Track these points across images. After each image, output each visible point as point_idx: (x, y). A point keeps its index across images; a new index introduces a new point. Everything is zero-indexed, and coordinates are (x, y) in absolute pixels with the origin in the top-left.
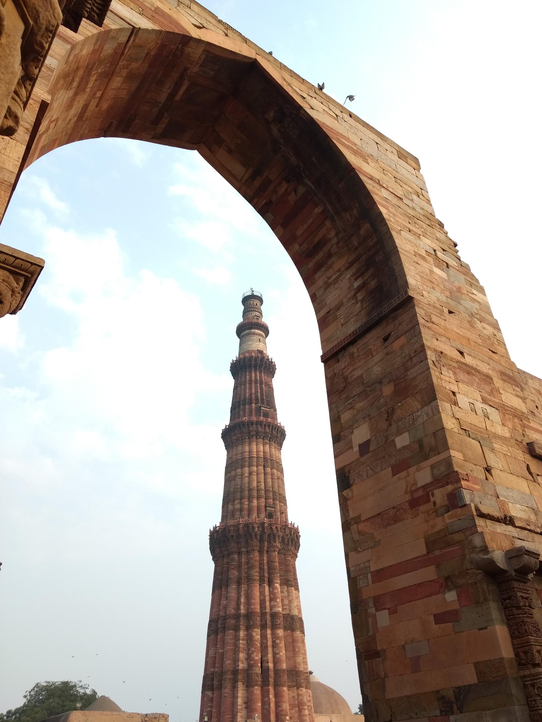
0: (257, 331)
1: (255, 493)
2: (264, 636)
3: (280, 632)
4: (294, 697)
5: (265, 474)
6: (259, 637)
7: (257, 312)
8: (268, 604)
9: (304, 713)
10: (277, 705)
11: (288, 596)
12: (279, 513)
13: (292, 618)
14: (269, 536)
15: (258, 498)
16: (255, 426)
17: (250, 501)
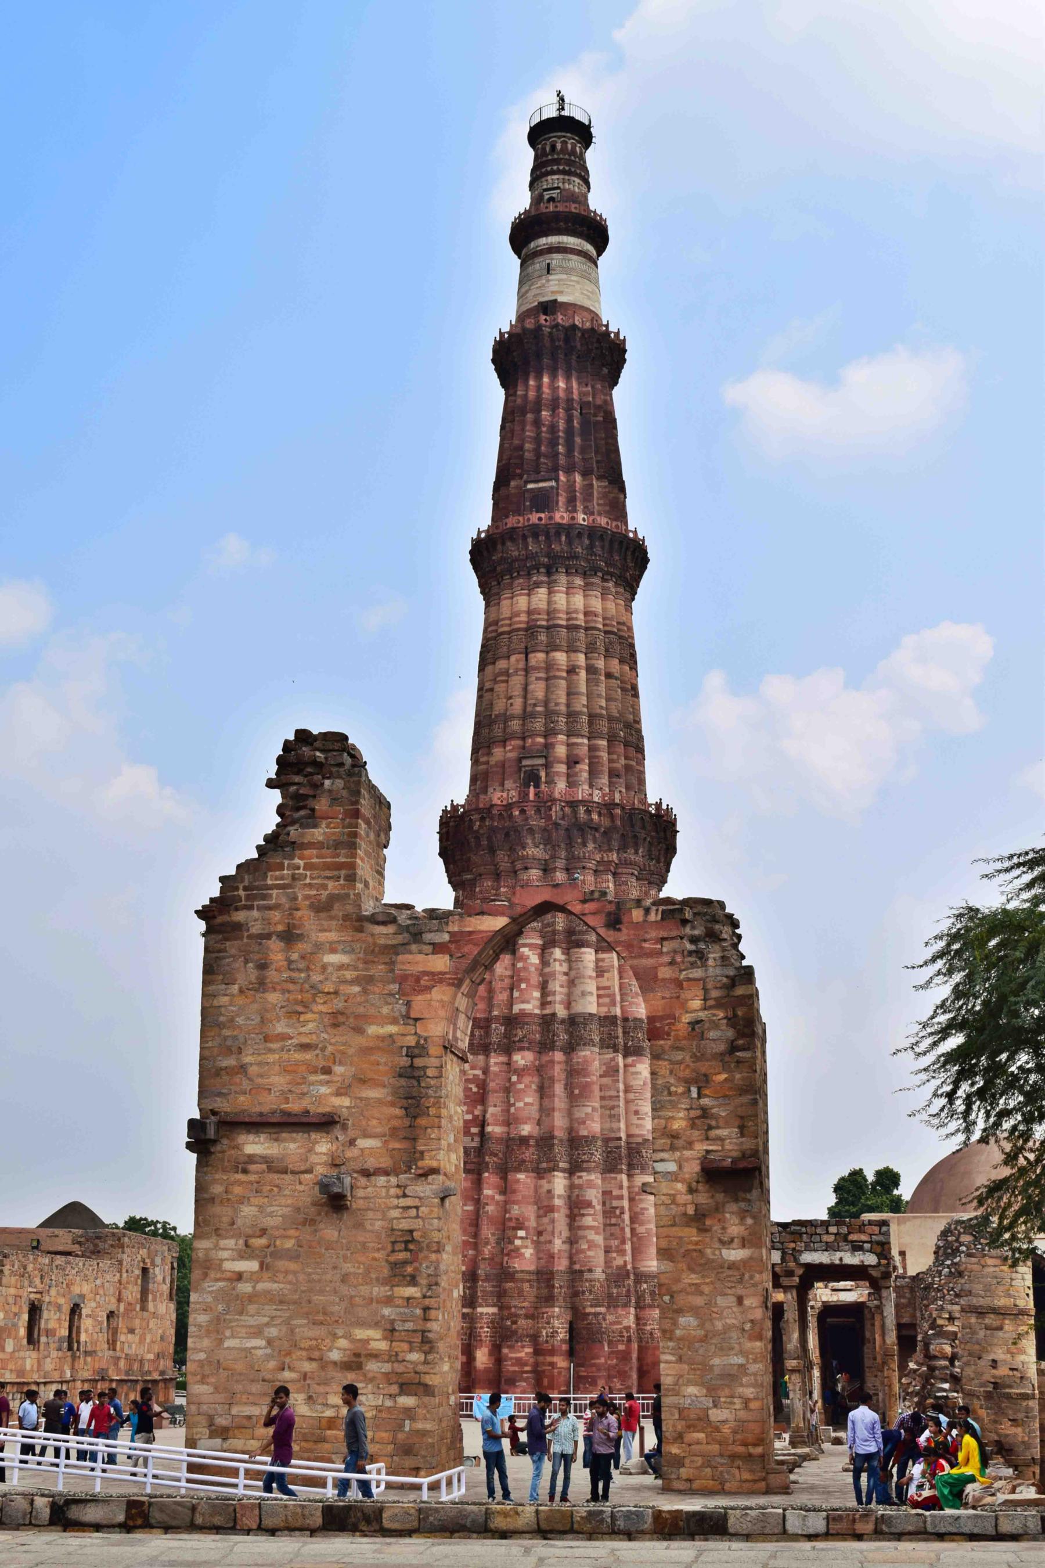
0: (543, 241)
1: (498, 731)
2: (486, 1071)
3: (521, 1059)
4: (549, 1191)
5: (527, 670)
6: (478, 1072)
7: (553, 173)
8: (502, 997)
9: (580, 1224)
10: (505, 1207)
11: (570, 968)
12: (562, 768)
13: (573, 1022)
14: (507, 835)
15: (504, 743)
16: (499, 547)
17: (489, 754)
